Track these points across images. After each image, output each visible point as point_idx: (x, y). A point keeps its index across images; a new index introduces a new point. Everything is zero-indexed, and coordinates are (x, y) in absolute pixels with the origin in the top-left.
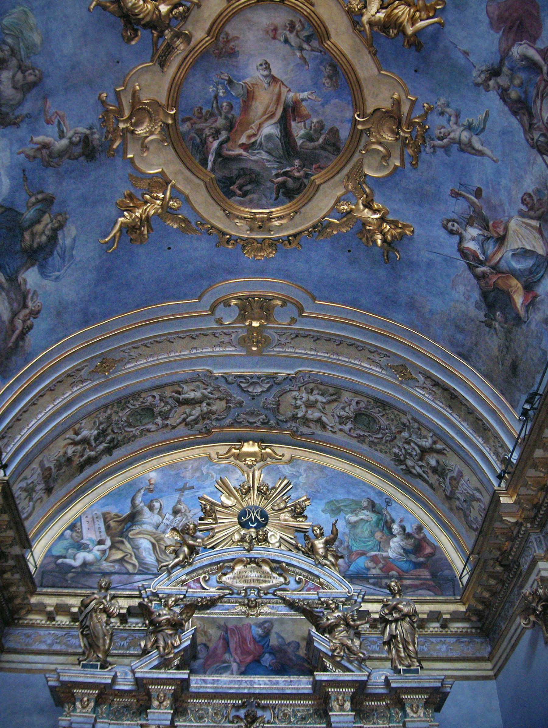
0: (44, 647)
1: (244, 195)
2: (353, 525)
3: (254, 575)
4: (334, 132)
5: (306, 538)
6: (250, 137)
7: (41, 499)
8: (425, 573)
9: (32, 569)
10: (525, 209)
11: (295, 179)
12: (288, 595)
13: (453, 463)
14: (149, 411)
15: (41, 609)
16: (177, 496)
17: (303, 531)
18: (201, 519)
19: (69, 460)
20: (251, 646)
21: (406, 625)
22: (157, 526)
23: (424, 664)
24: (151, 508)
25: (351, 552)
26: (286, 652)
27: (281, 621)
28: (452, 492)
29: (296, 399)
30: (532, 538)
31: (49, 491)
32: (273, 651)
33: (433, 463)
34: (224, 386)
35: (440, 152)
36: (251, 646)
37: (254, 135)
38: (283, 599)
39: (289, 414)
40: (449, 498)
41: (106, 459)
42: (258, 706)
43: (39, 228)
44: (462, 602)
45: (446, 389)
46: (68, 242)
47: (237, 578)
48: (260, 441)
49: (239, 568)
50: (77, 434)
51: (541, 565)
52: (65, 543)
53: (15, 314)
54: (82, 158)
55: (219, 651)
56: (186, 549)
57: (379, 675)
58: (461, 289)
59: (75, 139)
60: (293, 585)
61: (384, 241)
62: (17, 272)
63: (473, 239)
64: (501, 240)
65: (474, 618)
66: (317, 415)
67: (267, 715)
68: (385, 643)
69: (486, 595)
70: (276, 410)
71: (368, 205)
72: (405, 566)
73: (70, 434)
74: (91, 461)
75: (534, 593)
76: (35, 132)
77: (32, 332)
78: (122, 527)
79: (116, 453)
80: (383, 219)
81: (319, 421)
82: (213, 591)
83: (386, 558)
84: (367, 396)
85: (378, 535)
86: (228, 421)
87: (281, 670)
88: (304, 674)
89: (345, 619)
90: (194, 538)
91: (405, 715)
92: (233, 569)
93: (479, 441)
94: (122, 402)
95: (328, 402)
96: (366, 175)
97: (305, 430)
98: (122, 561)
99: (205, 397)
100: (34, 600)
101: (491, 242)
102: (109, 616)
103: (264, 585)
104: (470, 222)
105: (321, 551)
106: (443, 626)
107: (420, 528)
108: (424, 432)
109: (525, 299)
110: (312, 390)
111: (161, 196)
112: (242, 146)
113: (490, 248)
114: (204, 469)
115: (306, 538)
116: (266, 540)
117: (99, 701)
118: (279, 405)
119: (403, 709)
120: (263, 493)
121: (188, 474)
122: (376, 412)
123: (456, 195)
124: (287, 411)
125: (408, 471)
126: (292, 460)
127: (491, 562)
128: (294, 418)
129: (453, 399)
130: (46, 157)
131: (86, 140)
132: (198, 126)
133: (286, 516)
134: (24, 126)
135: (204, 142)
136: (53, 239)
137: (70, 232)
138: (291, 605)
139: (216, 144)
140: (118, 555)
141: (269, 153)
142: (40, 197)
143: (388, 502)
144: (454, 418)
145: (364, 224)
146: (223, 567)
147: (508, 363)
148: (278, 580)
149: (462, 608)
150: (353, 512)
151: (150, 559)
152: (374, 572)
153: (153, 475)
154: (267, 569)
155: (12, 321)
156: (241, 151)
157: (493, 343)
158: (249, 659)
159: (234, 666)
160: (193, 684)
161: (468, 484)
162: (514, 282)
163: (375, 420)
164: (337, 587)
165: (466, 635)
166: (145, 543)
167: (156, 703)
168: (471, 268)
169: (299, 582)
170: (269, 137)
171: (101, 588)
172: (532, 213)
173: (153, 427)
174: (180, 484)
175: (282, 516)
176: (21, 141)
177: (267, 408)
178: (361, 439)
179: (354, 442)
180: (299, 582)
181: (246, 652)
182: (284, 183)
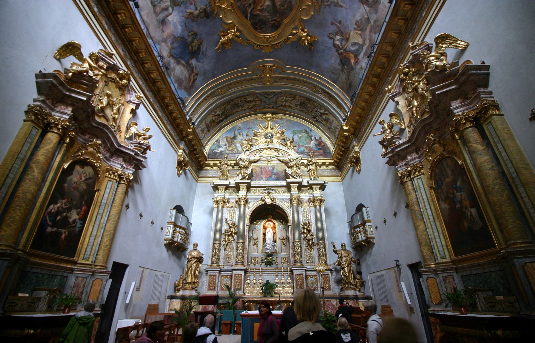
0: (210, 176)
1: (261, 29)
2: (300, 138)
4: (290, 2)
6: (261, 6)
7: (206, 133)
8: (322, 151)
9: (205, 154)
10: (356, 27)
11: (278, 22)
12: (279, 158)
13: (331, 118)
14: (237, 105)
15: (208, 165)
16: (247, 131)
19: (214, 121)
20: (269, 173)
22: (242, 140)
23: (320, 178)
24: (240, 135)
25: (299, 146)
27: (278, 165)
28: (330, 126)
31: (209, 131)
32: (275, 174)
33: (324, 118)
34: (259, 96)
35: (327, 7)
36: (269, 173)
37: (263, 6)
38: (278, 160)
39: (280, 104)
40: (329, 128)
41: (225, 120)
43: (194, 44)
44: (333, 159)
45: (328, 93)
46: (204, 49)
48: (272, 113)
50: (215, 113)
51: (356, 147)
52: (215, 146)
53: (190, 75)
54: (205, 18)
56: (249, 146)
57: (305, 181)
58: (334, 59)
59: (201, 10)
60: (281, 155)
61: (308, 43)
62: (189, 60)
63: (338, 40)
64: (347, 40)
65: (336, 164)
66: (289, 104)
67: (274, 192)
69: (339, 157)
70: (276, 103)
71: (303, 30)
72: (315, 149)
73: (213, 113)
74: (221, 121)
75: (353, 156)
76: (186, 8)
77: (197, 81)
78: (231, 140)
79: (228, 118)
80: (308, 35)
81: (289, 106)
82: (257, 158)
83: (310, 147)
84: (304, 97)
85: (308, 140)
86: (262, 107)
87: (277, 179)
89: (296, 164)
90: (251, 142)
92: (263, 151)
93: (338, 110)
94: (228, 102)
95: (292, 100)
96: (302, 19)
97: (285, 109)
98: (232, 150)
99: (254, 100)
100: (206, 162)
101: (344, 41)
102: (228, 165)
104: (337, 34)
106: (327, 167)
107: (320, 138)
108: (322, 108)
109: (355, 61)
111: (233, 31)
112: (259, 10)
113: (344, 43)
114: (255, 122)
117: (226, 189)
120: (272, 129)
121: (250, 124)
122: (306, 102)
123: (332, 24)
124: (279, 104)
125: (317, 121)
126: (281, 119)
127: (341, 147)
128: (282, 105)
129: (331, 97)
130: (191, 17)
131: (205, 10)
132: (243, 3)
134: (182, 6)
135: (246, 9)
136: (199, 48)
137: (205, 46)
139: (250, 10)
140: (231, 149)
141: (268, 12)
142: (192, 33)
143: (311, 130)
144: (331, 103)
145: (301, 37)
147: (348, 83)
148: (276, 154)
149: (332, 161)
150: (300, 133)
151: (240, 149)
152: (306, 151)
153: (240, 125)
154: (273, 150)
155: (189, 77)
156: (258, 12)
157: (343, 77)
159: (264, 178)
161: (335, 123)
162: (352, 55)
163: (307, 105)
164: (293, 155)
165: (333, 169)
166: (238, 145)
167: (241, 189)
168: (337, 51)
170: (268, 6)
172: (358, 28)
173: (239, 110)
174: (248, 127)
176: (182, 11)
178: (302, 111)
179: (301, 112)
181: (267, 174)
182: (274, 24)
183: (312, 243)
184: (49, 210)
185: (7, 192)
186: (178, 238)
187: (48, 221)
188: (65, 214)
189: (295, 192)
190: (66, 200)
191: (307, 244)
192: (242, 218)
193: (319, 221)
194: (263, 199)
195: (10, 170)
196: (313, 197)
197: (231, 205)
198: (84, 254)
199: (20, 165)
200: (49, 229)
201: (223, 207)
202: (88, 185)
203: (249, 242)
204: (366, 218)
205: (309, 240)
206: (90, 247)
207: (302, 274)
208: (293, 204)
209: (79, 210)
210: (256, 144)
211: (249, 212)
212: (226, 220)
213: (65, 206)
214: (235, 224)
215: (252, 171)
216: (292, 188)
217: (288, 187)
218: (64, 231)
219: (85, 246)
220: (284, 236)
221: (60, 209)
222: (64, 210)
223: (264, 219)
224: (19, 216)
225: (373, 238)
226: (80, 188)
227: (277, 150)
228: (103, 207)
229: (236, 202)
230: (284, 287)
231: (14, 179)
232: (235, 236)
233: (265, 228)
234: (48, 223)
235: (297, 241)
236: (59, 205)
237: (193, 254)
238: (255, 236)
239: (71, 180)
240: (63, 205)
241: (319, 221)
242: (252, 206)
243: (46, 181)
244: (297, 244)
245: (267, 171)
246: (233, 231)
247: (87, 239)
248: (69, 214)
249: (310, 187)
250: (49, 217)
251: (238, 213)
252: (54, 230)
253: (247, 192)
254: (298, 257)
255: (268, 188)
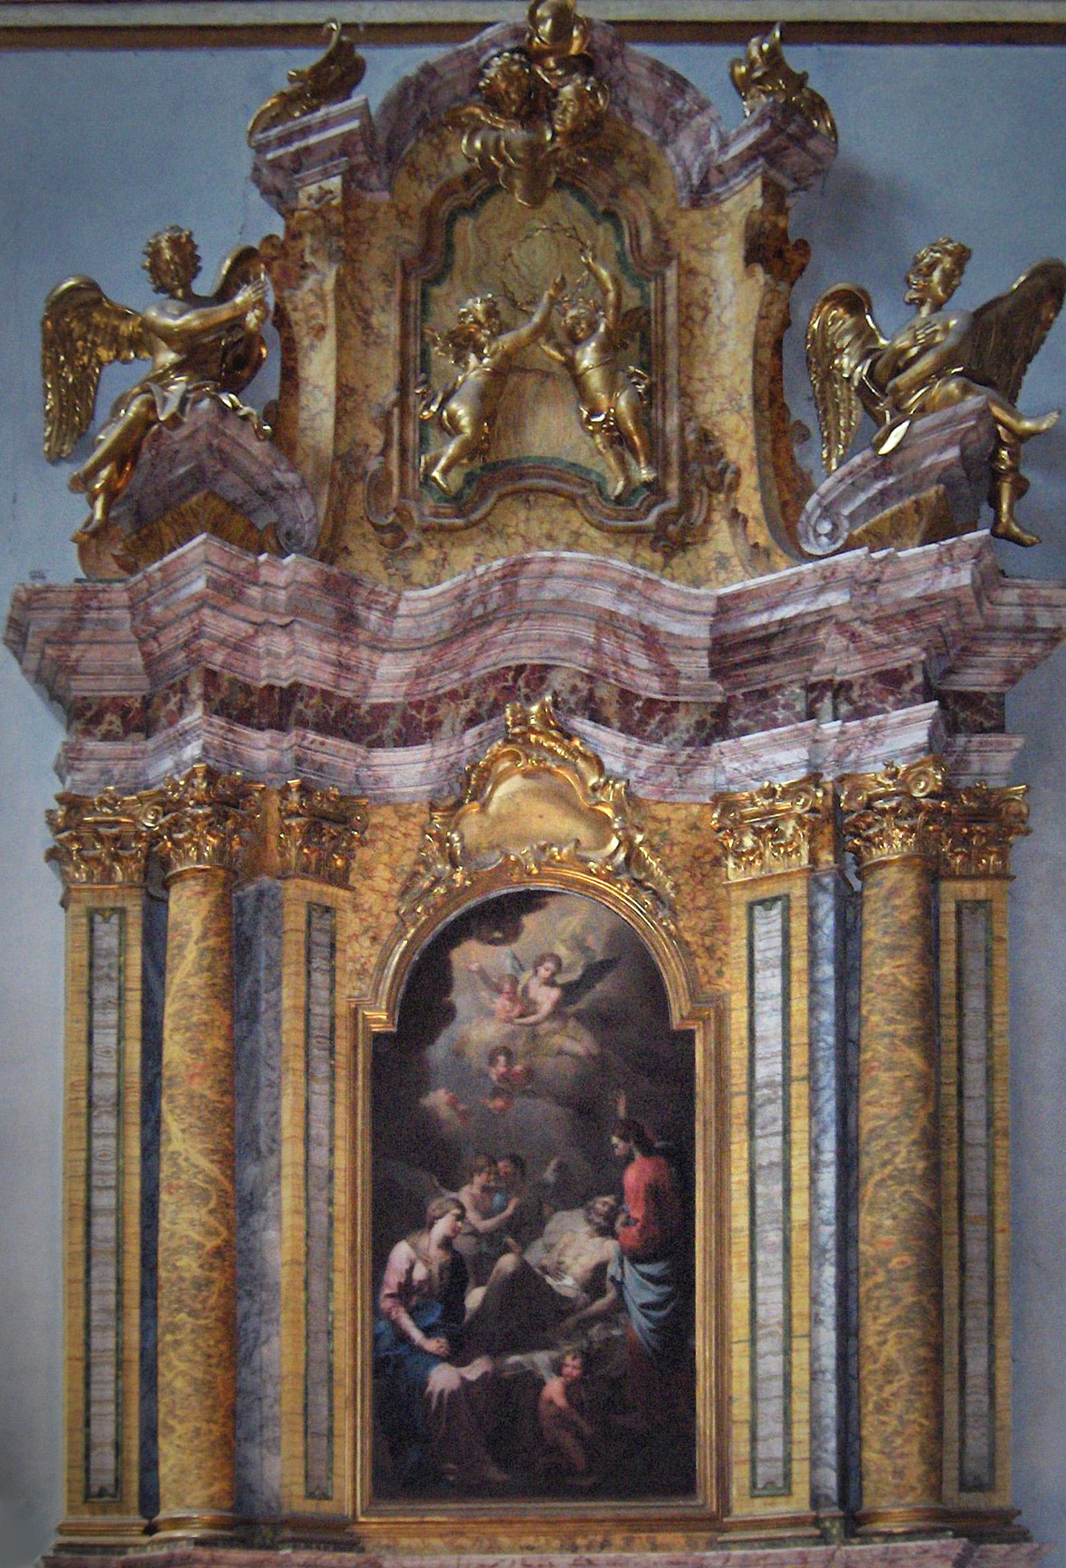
184: (393, 1278)
185: (120, 1281)
187: (417, 1335)
188: (507, 1262)
190: (479, 1180)
195: (88, 1175)
198: (753, 1462)
199: (120, 1135)
200: (443, 1378)
202: (601, 1021)
206: (771, 1409)
209: (603, 1203)
213: (487, 1215)
218: (542, 1359)
219: (740, 1410)
221: (463, 1244)
222: (494, 1243)
224: (183, 1374)
226: (547, 1064)
228: (775, 1110)
231: (119, 1208)
234: (420, 1350)
236: (442, 1228)
239: (458, 1053)
240: (472, 1215)
243: (275, 1141)
247: (739, 1363)
248: (536, 1255)
250: (412, 1313)
252: (476, 1369)
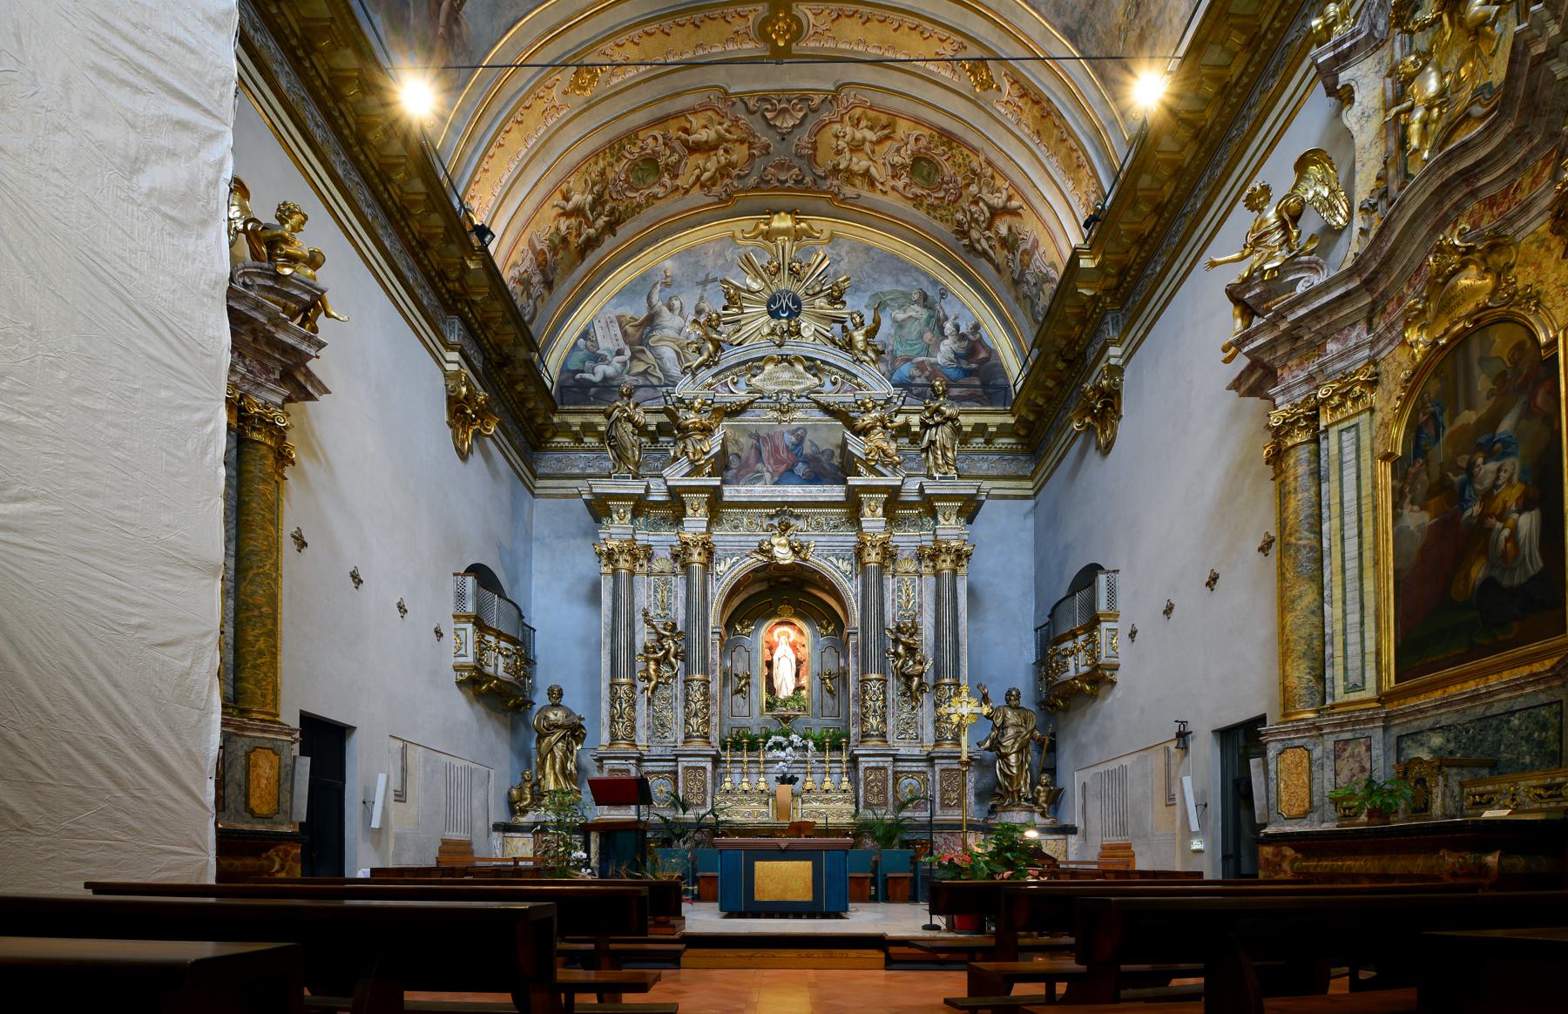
3: (786, 376)
5: (845, 329)
17: (841, 321)
18: (725, 308)
20: (784, 455)
21: (947, 429)
26: (819, 460)
27: (815, 428)
29: (837, 137)
30: (1109, 318)
32: (807, 461)
42: (792, 515)
47: (772, 379)
49: (769, 367)
55: (752, 461)
60: (828, 387)
67: (801, 524)
68: (922, 450)
70: (812, 159)
82: (742, 395)
87: (814, 478)
88: (837, 483)
91: (937, 522)
103: (797, 387)
105: (860, 345)
110: (859, 120)
115: (845, 329)
116: (798, 333)
117: (636, 513)
118: (815, 149)
119: (935, 518)
124: (826, 160)
133: (821, 302)
138: (826, 409)
146: (753, 366)
154: (799, 367)
158: (783, 468)
159: (767, 476)
160: (726, 493)
169: (834, 384)
171: (622, 395)
175: (818, 302)
177: (801, 157)
180: (834, 384)
181: (778, 462)
183: (921, 684)
186: (498, 666)
189: (873, 521)
191: (903, 687)
192: (696, 605)
193: (947, 620)
194: (766, 546)
196: (936, 541)
197: (657, 567)
201: (632, 573)
203: (724, 685)
204: (1102, 606)
205: (909, 678)
207: (884, 768)
208: (864, 565)
210: (736, 339)
211: (717, 592)
212: (646, 614)
214: (674, 625)
215: (724, 445)
216: (866, 510)
217: (852, 507)
220: (831, 666)
223: (768, 617)
225: (1115, 668)
227: (813, 366)
229: (675, 557)
230: (829, 801)
232: (679, 665)
233: (772, 648)
235: (874, 676)
237: (552, 716)
238: (740, 668)
241: (947, 620)
242: (728, 570)
244: (874, 687)
245: (776, 450)
246: (673, 648)
249: (929, 506)
251: (682, 593)
253: (710, 523)
254: (874, 722)
255: (783, 514)
